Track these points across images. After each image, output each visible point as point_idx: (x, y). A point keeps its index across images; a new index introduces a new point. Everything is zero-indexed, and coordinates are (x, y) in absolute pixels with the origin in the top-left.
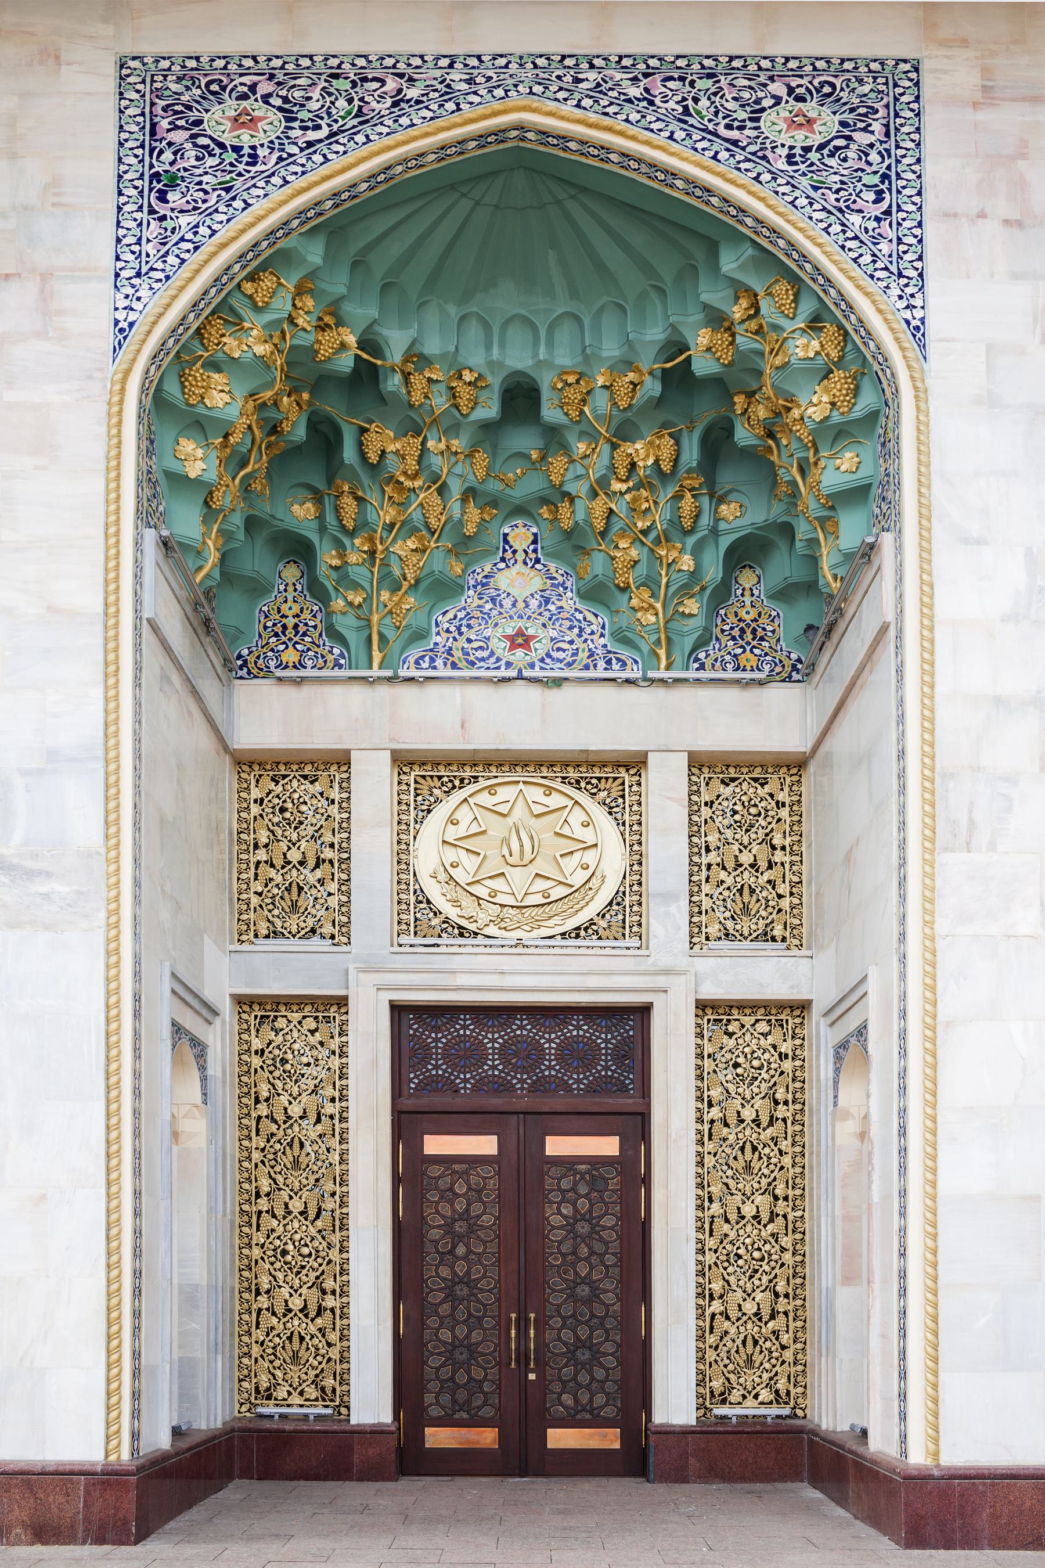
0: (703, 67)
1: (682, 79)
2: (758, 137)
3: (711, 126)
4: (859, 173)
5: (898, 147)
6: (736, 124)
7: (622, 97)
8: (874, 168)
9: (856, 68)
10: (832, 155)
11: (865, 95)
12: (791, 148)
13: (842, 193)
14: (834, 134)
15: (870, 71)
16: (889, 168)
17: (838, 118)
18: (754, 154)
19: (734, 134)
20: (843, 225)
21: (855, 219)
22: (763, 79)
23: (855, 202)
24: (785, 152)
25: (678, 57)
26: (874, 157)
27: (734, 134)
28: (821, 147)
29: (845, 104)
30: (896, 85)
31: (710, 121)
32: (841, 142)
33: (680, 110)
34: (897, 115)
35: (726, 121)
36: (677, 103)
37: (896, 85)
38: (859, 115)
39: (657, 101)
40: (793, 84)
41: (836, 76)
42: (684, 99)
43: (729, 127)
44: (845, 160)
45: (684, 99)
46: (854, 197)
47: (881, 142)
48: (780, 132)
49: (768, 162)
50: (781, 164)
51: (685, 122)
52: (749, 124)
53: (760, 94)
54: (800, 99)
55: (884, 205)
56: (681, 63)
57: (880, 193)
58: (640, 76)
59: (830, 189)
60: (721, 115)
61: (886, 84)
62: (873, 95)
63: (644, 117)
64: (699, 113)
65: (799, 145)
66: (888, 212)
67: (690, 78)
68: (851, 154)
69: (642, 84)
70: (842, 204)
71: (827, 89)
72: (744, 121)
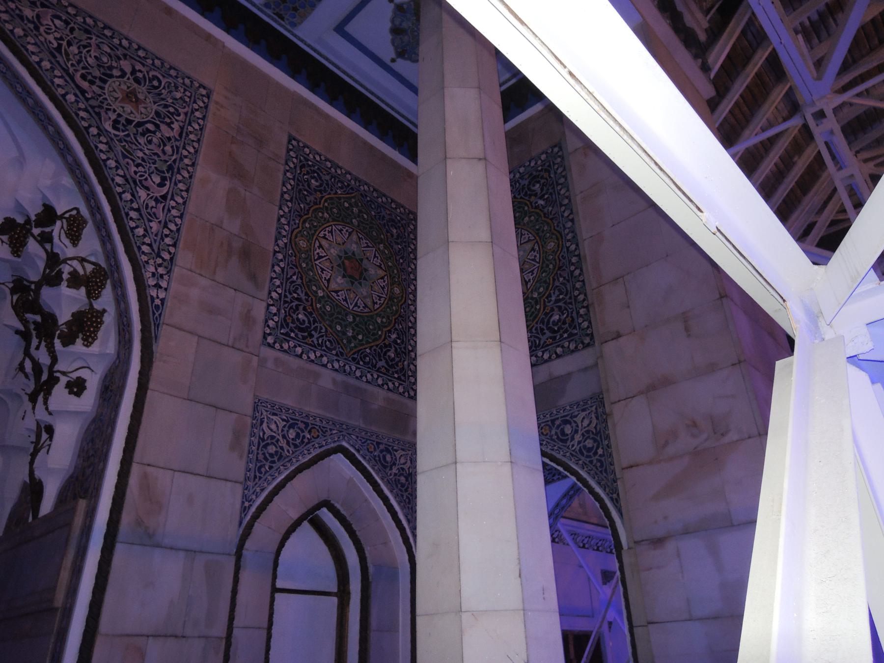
0: (85, 22)
1: (67, 23)
2: (100, 96)
3: (71, 70)
4: (156, 158)
5: (184, 148)
6: (89, 77)
7: (17, 12)
8: (166, 158)
9: (177, 77)
10: (143, 134)
11: (176, 99)
12: (119, 115)
13: (140, 169)
14: (149, 118)
15: (184, 83)
16: (175, 161)
17: (155, 107)
18: (93, 107)
19: (85, 85)
20: (133, 195)
21: (142, 193)
22: (119, 53)
23: (146, 179)
24: (113, 116)
25: (71, 5)
26: (168, 149)
27: (85, 85)
28: (139, 124)
29: (163, 99)
30: (195, 102)
31: (72, 65)
32: (150, 127)
33: (55, 45)
34: (190, 124)
35: (84, 71)
36: (56, 39)
37: (195, 102)
38: (169, 112)
39: (42, 29)
40: (137, 68)
41: (164, 77)
42: (61, 39)
43: (83, 77)
44: (150, 142)
45: (61, 39)
46: (147, 175)
47: (176, 140)
48: (116, 99)
49: (100, 119)
50: (108, 126)
51: (55, 57)
52: (98, 82)
53: (115, 64)
54: (137, 81)
55: (164, 190)
56: (71, 10)
57: (164, 179)
58: (38, 4)
59: (134, 161)
60: (82, 65)
61: (190, 97)
62: (181, 102)
63: (26, 36)
64: (67, 54)
65: (125, 116)
66: (164, 197)
67: (72, 25)
68: (155, 140)
69: (37, 10)
70: (137, 177)
71: (155, 83)
72: (95, 77)
